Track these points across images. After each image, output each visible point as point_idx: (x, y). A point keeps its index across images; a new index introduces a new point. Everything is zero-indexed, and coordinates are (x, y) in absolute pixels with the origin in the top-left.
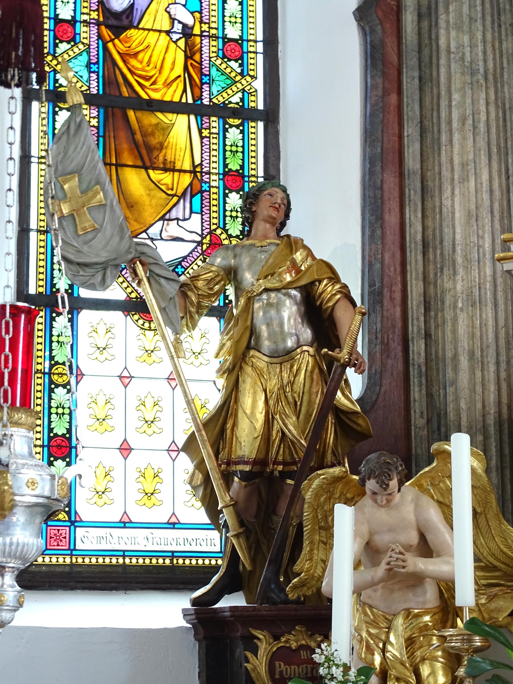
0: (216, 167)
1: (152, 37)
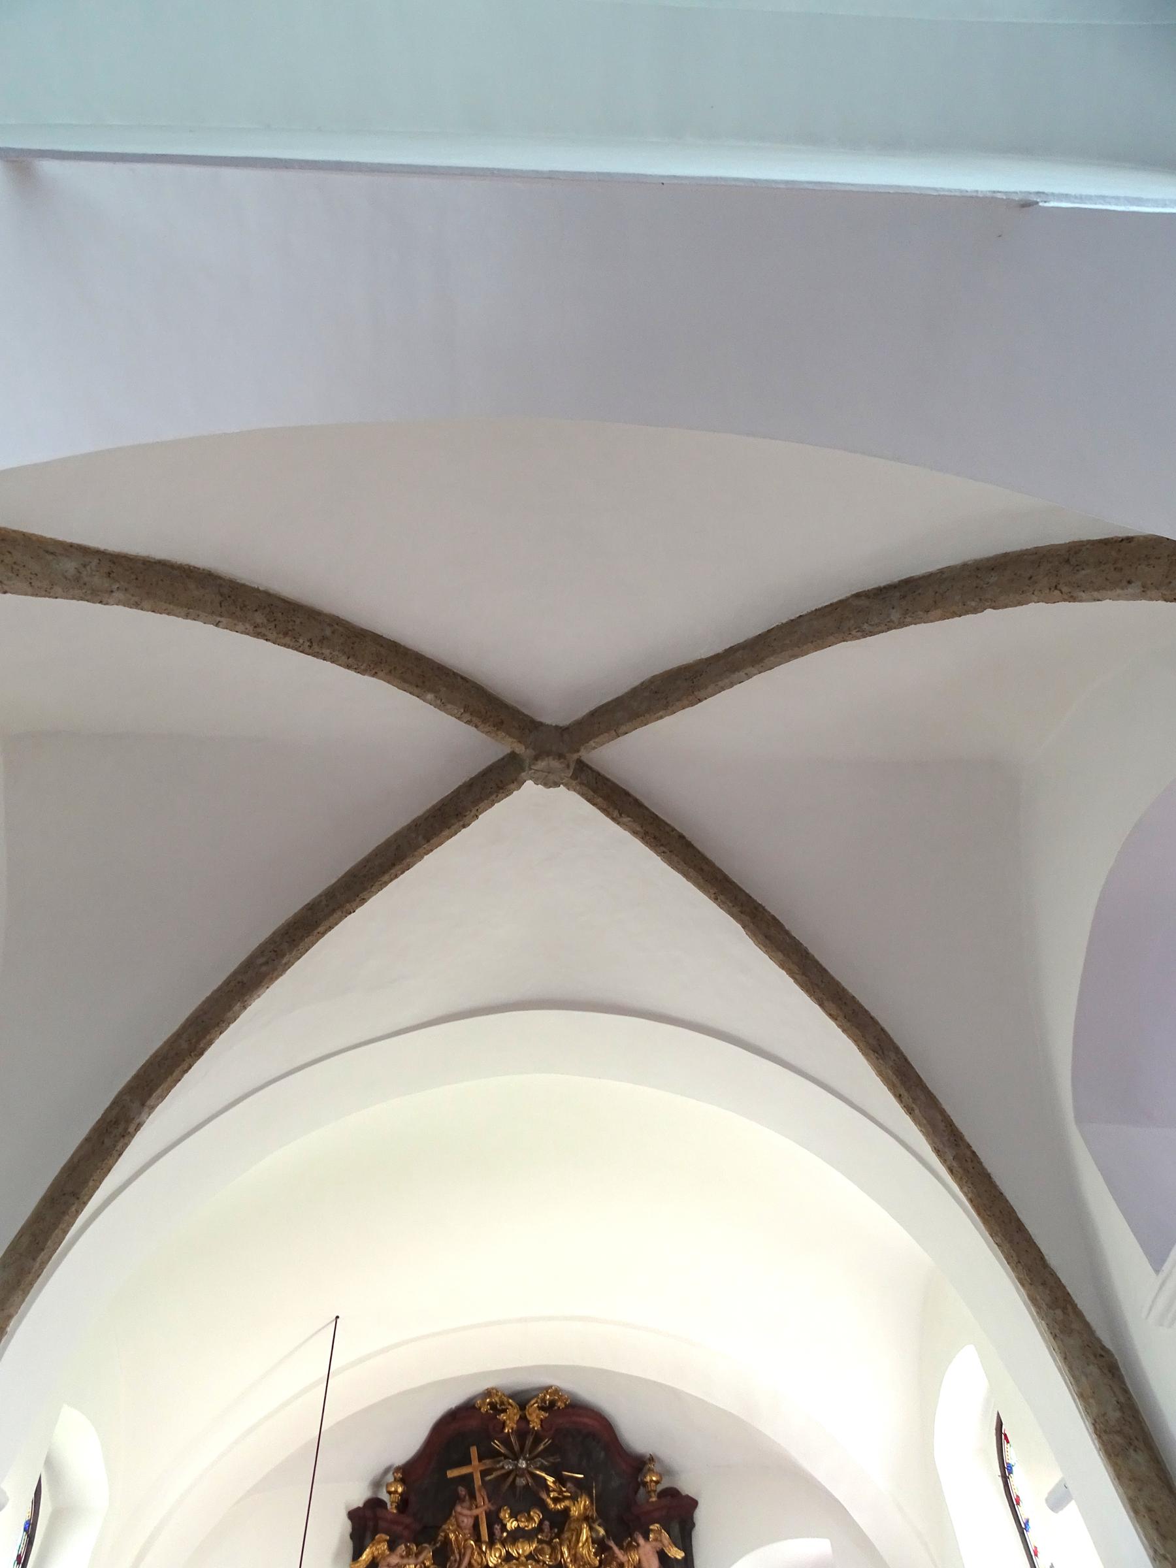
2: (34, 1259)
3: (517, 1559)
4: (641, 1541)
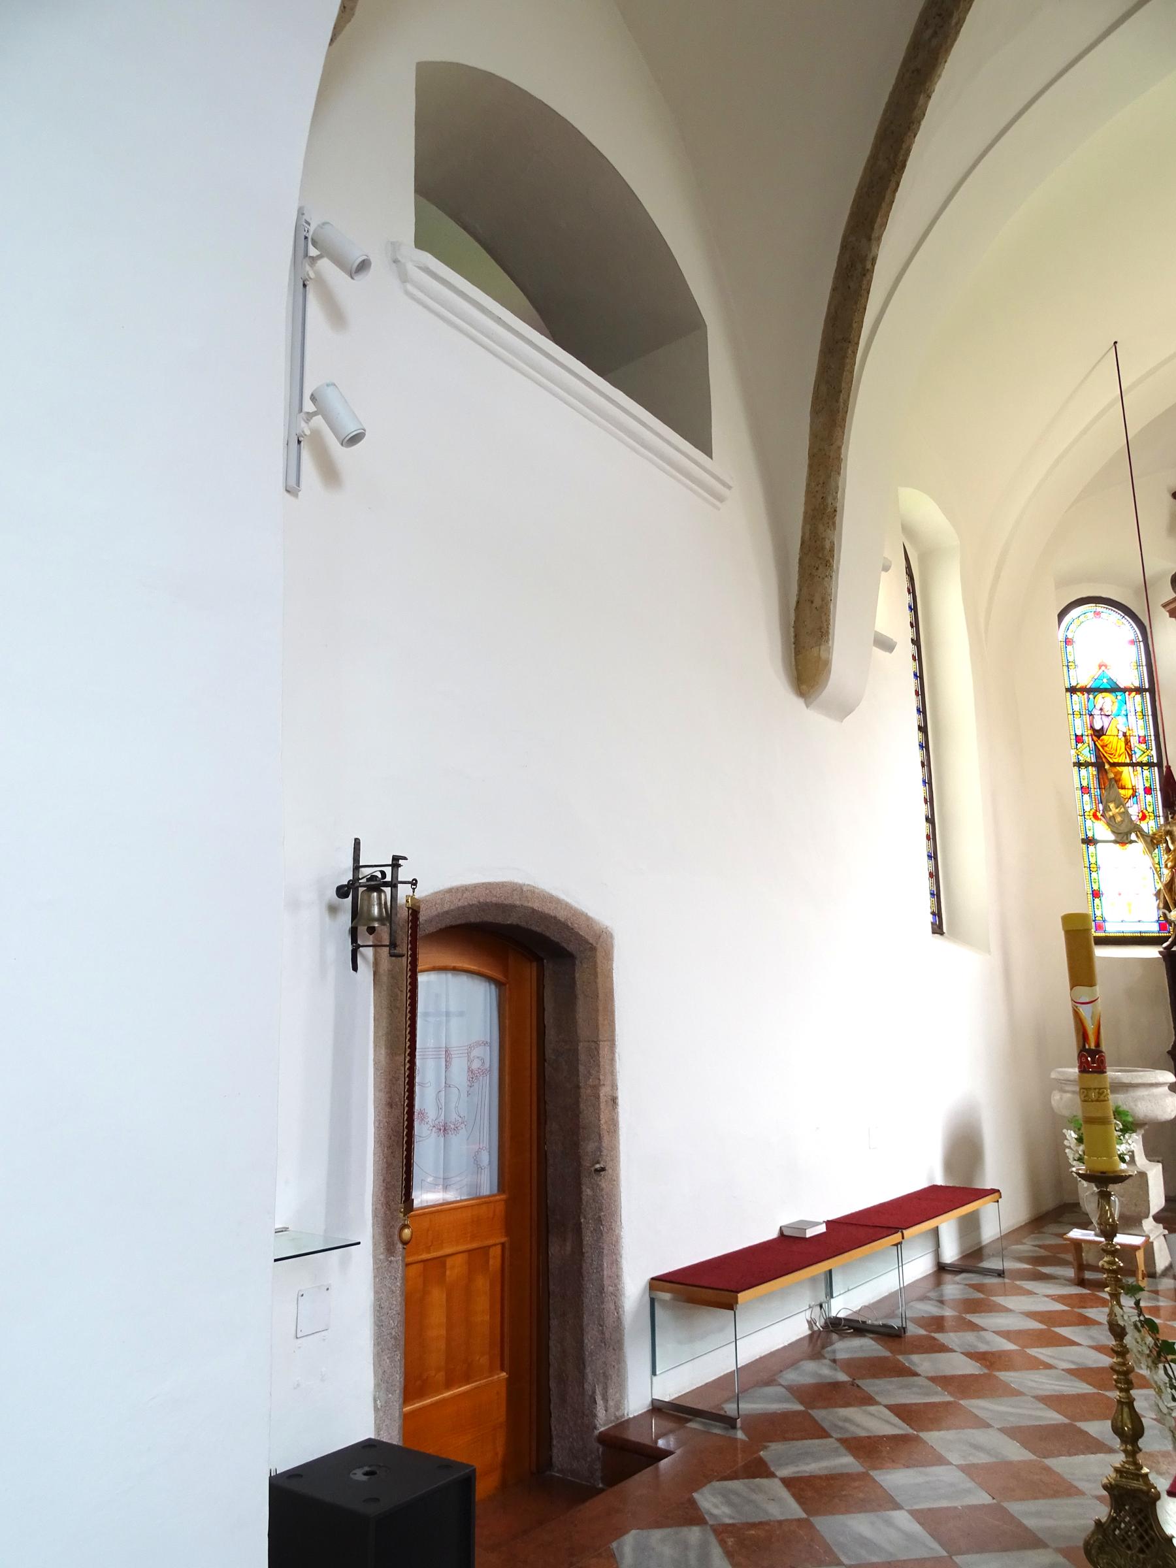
1: (1112, 738)
2: (837, 401)
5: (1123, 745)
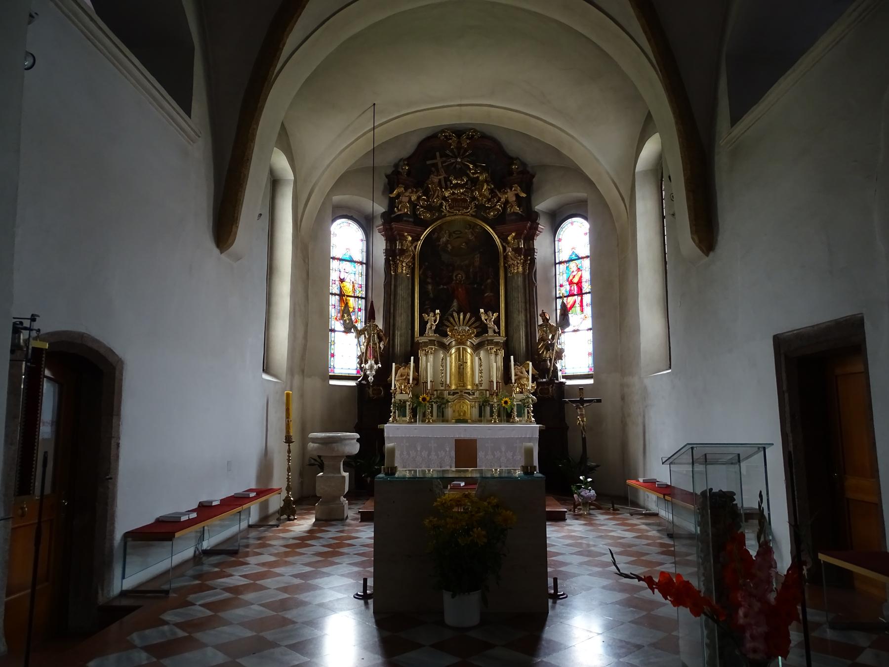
0: (357, 308)
3: (457, 194)
4: (509, 190)
5: (351, 287)
